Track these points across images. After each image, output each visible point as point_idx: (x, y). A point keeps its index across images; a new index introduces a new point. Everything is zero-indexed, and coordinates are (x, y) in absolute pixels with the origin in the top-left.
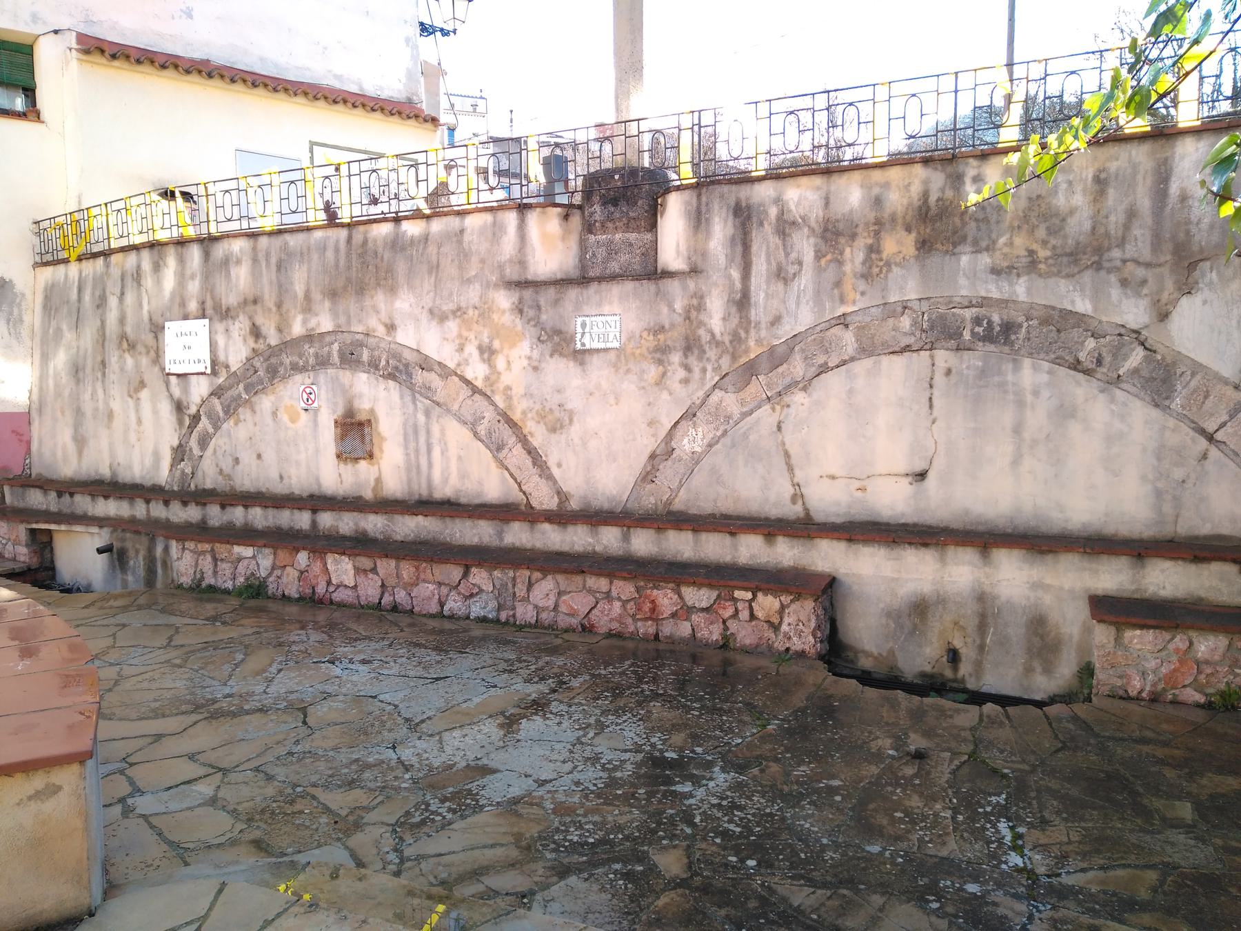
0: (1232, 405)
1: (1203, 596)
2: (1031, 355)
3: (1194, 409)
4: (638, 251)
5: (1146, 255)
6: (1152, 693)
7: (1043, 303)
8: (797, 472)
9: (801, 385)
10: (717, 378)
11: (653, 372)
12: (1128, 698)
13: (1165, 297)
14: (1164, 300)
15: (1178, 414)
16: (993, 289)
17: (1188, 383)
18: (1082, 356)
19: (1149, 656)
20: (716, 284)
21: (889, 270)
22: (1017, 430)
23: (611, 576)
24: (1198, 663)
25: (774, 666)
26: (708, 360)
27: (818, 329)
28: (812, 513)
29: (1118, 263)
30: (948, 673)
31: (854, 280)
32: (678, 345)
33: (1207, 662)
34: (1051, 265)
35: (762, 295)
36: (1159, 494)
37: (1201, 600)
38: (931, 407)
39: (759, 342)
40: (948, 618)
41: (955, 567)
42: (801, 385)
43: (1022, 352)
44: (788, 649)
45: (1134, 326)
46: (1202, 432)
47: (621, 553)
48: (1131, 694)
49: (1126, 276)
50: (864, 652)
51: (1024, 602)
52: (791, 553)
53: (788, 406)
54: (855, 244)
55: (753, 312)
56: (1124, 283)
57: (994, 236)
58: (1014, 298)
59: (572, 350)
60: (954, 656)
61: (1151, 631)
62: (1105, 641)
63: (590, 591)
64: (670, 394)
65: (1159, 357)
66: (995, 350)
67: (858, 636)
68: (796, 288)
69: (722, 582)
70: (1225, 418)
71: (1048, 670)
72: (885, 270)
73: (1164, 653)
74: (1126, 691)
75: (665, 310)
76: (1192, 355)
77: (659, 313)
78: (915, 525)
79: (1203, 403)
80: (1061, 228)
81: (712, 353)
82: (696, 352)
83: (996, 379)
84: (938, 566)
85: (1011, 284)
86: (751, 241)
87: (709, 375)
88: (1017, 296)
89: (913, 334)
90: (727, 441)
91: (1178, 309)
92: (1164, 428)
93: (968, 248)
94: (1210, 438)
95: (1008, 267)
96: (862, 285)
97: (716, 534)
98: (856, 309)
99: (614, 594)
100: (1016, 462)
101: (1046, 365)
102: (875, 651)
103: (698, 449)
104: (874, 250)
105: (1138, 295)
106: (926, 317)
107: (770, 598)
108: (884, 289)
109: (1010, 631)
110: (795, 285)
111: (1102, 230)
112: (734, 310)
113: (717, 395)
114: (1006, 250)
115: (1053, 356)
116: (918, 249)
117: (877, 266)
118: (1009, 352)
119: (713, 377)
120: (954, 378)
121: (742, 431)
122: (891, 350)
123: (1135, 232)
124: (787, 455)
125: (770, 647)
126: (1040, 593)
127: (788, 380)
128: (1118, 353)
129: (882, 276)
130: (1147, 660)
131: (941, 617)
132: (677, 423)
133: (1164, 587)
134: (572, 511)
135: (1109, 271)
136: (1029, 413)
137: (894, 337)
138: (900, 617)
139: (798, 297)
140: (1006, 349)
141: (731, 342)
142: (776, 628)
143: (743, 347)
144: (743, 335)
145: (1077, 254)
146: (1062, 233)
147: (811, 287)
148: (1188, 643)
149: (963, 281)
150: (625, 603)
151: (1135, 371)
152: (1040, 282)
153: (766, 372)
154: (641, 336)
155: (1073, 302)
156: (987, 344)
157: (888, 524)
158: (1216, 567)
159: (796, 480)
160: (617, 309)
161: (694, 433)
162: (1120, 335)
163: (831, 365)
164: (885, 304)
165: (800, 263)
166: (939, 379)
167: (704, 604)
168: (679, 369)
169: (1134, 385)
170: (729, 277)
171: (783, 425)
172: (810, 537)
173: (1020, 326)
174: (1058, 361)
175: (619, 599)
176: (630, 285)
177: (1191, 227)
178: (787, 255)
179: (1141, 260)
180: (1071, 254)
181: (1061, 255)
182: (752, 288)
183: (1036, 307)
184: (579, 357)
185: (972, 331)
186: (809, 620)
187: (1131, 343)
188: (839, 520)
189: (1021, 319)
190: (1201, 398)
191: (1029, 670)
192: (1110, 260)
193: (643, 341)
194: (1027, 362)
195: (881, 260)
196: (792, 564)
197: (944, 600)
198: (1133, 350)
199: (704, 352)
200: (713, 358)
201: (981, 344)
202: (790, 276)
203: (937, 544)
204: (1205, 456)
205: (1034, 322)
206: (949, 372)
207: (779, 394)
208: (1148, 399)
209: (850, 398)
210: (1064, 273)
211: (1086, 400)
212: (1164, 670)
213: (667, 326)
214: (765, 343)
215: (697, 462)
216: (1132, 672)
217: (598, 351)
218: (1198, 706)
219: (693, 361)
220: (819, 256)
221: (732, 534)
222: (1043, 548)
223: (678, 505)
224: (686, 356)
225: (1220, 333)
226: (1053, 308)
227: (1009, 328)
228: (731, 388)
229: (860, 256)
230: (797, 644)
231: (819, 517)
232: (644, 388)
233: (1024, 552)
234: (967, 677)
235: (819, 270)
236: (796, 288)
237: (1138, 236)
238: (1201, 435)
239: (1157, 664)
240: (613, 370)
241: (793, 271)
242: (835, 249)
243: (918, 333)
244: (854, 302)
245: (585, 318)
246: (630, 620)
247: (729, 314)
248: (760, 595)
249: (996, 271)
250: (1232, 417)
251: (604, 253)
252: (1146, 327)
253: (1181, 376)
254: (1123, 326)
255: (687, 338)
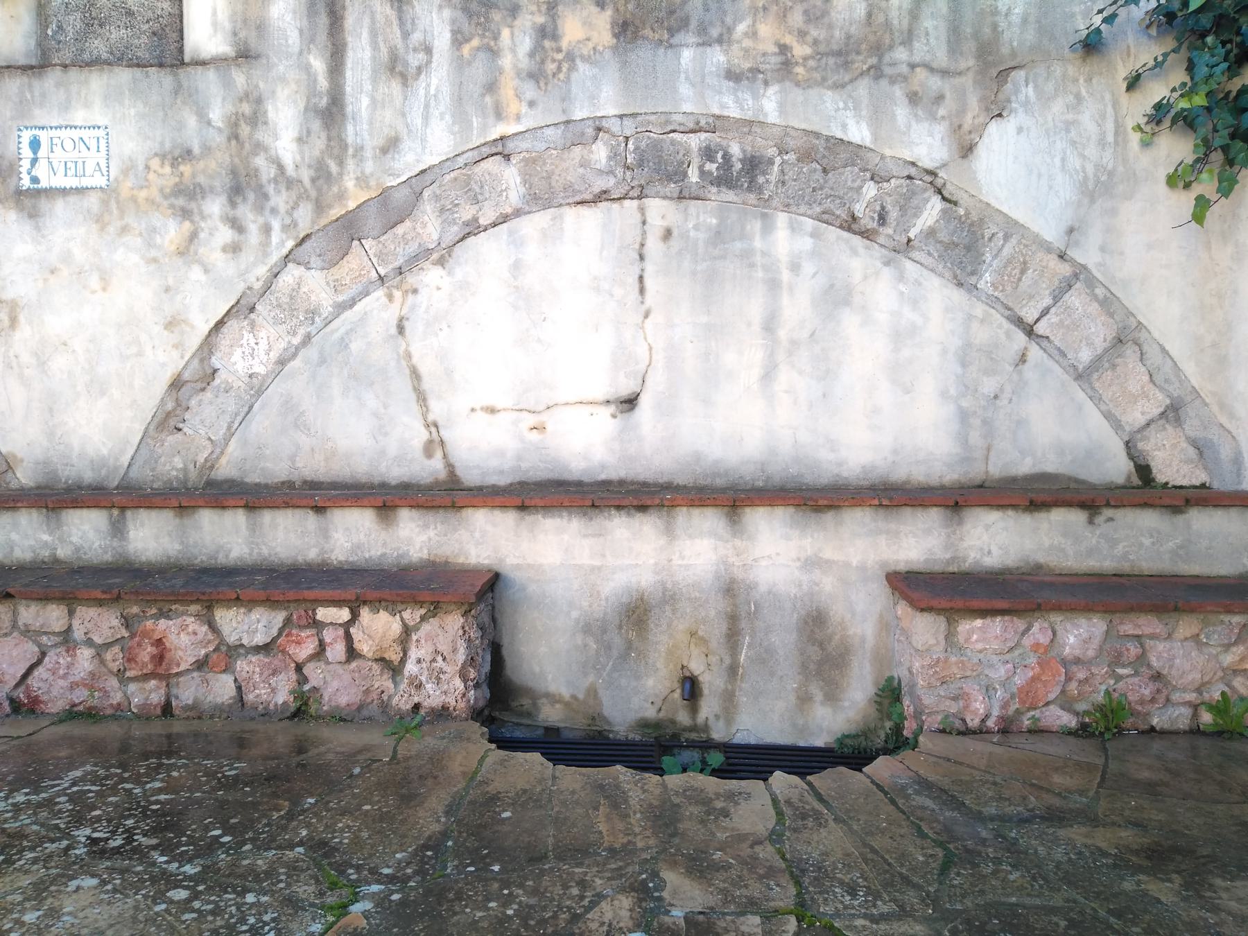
0: (1057, 283)
1: (1042, 560)
2: (787, 207)
3: (1009, 289)
4: (146, 27)
5: (941, 58)
6: (1002, 718)
7: (803, 126)
8: (433, 404)
9: (435, 256)
10: (290, 244)
11: (172, 231)
12: (966, 732)
13: (968, 121)
14: (966, 127)
15: (988, 296)
16: (730, 104)
17: (1000, 250)
18: (859, 209)
19: (995, 659)
20: (283, 80)
21: (573, 68)
22: (769, 326)
23: (70, 600)
24: (1064, 662)
25: (389, 743)
26: (274, 211)
27: (461, 161)
28: (459, 472)
29: (904, 69)
30: (683, 718)
31: (516, 82)
32: (217, 183)
33: (1077, 661)
34: (812, 69)
35: (365, 101)
36: (964, 416)
37: (1039, 567)
38: (642, 291)
39: (362, 181)
40: (682, 626)
41: (688, 542)
42: (435, 256)
43: (775, 203)
44: (417, 707)
45: (928, 164)
46: (1019, 322)
47: (108, 557)
48: (970, 724)
49: (916, 88)
50: (547, 695)
51: (794, 591)
52: (424, 538)
53: (415, 291)
54: (517, 23)
55: (350, 129)
56: (914, 99)
57: (729, 20)
58: (761, 119)
59: (12, 188)
60: (691, 688)
61: (998, 619)
62: (933, 641)
63: (27, 632)
64: (206, 271)
65: (962, 212)
66: (735, 199)
67: (537, 669)
68: (422, 92)
69: (291, 595)
70: (1047, 301)
71: (832, 697)
72: (565, 67)
73: (1017, 652)
74: (964, 720)
75: (192, 121)
76: (1005, 209)
77: (181, 126)
78: (622, 482)
79: (1020, 279)
80: (825, 13)
81: (280, 200)
82: (251, 196)
83: (738, 245)
84: (662, 541)
85: (756, 97)
86: (344, 8)
87: (276, 237)
88: (766, 115)
89: (611, 172)
90: (311, 352)
91: (985, 139)
92: (970, 317)
93: (691, 39)
94: (1029, 331)
95: (751, 70)
96: (530, 91)
97: (289, 512)
98: (521, 128)
99: (78, 634)
100: (768, 376)
101: (809, 223)
102: (566, 693)
103: (260, 369)
104: (547, 33)
105: (933, 117)
106: (631, 146)
107: (383, 616)
108: (566, 98)
109: (774, 639)
110: (421, 86)
111: (881, 18)
112: (316, 125)
113: (292, 274)
114: (747, 43)
115: (818, 209)
116: (616, 36)
117: (554, 61)
118: (755, 202)
119: (283, 243)
120: (675, 243)
121: (337, 335)
122: (578, 199)
123: (926, 24)
124: (415, 374)
125: (385, 706)
126: (817, 574)
127: (412, 248)
128: (908, 207)
129: (561, 76)
130: (992, 666)
131: (669, 626)
132: (220, 324)
133: (989, 552)
134: (22, 489)
135: (893, 80)
136: (785, 300)
137: (583, 177)
138: (604, 631)
139: (427, 106)
140: (752, 198)
141: (313, 180)
142: (394, 669)
143: (335, 189)
144: (333, 167)
145: (847, 53)
146: (826, 20)
147: (446, 90)
148: (1050, 632)
149: (685, 90)
150: (100, 650)
151: (931, 233)
152: (797, 95)
153: (375, 233)
154: (147, 167)
155: (844, 126)
156: (724, 189)
157: (579, 484)
158: (1058, 516)
159: (431, 418)
160: (99, 116)
161: (252, 341)
162: (909, 177)
163: (483, 221)
164: (568, 122)
165: (428, 50)
166: (654, 245)
167: (260, 639)
168: (221, 226)
169: (929, 254)
170: (307, 68)
171: (406, 324)
172: (455, 507)
173: (771, 162)
174: (825, 218)
175: (89, 643)
176: (124, 75)
177: (998, 18)
178: (406, 35)
179: (935, 65)
180: (839, 53)
181: (827, 54)
182: (348, 89)
183: (793, 133)
184: (27, 202)
185: (701, 168)
186: (455, 650)
187: (925, 190)
188: (503, 481)
189: (772, 152)
190: (1017, 271)
191: (804, 700)
192: (893, 64)
193: (151, 176)
194: (782, 219)
195: (559, 50)
196: (424, 555)
197: (673, 597)
198: (927, 200)
199: (266, 197)
200: (283, 208)
201: (714, 189)
202: (413, 71)
203: (661, 506)
204: (1023, 359)
205: (791, 157)
206: (668, 234)
207: (400, 271)
208: (948, 274)
209: (515, 278)
210: (830, 82)
211: (865, 278)
212: (1019, 680)
213: (196, 150)
214: (373, 183)
215: (260, 393)
216: (973, 689)
217: (64, 192)
218: (1071, 733)
219: (245, 212)
220: (459, 39)
221: (319, 509)
222: (821, 502)
223: (226, 469)
224: (233, 204)
225: (1040, 176)
226: (817, 135)
227: (754, 165)
228: (315, 261)
229: (526, 44)
230: (433, 696)
231: (470, 477)
232: (155, 260)
233: (791, 510)
234: (711, 722)
235: (460, 64)
236: (422, 92)
237: (931, 30)
238: (1019, 327)
239: (1007, 671)
240: (95, 227)
241: (416, 63)
242: (485, 30)
243: (619, 171)
244: (518, 118)
245: (37, 132)
246: (114, 682)
247: (309, 132)
248: (365, 613)
249: (733, 76)
250: (1056, 299)
251: (79, 25)
252: (944, 165)
253: (990, 239)
254: (913, 164)
255: (234, 172)
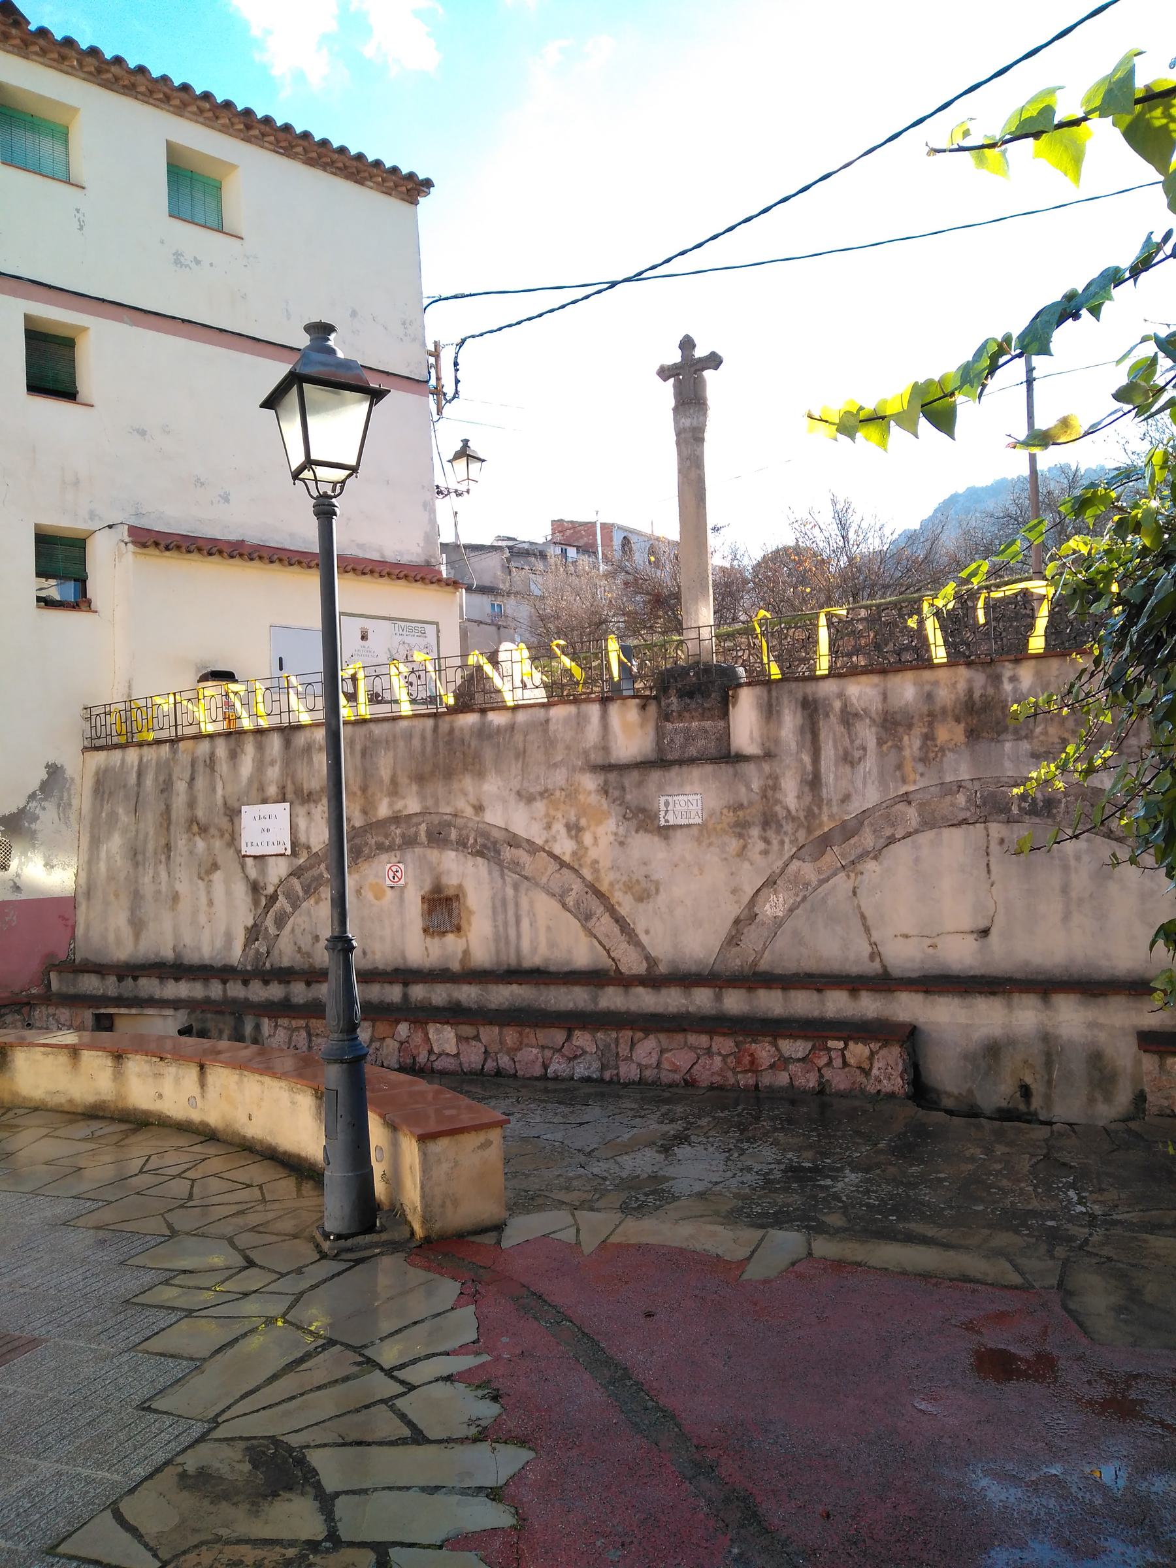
10: (794, 850)
11: (734, 844)
21: (944, 755)
22: (1065, 890)
23: (711, 1033)
26: (786, 833)
27: (884, 805)
30: (1022, 1107)
35: (832, 776)
38: (989, 872)
39: (831, 817)
44: (879, 1091)
47: (714, 1012)
50: (946, 1093)
52: (874, 1006)
53: (862, 873)
55: (824, 790)
60: (1026, 1091)
62: (1152, 1068)
63: (692, 1048)
64: (752, 864)
66: (1040, 822)
67: (939, 1078)
71: (1108, 1098)
74: (1173, 1110)
75: (743, 790)
78: (983, 977)
81: (788, 827)
82: (774, 826)
87: (787, 846)
89: (968, 809)
90: (807, 905)
93: (1010, 737)
95: (1045, 752)
96: (920, 768)
99: (715, 1049)
100: (1066, 917)
102: (956, 1091)
103: (780, 914)
104: (929, 737)
108: (941, 771)
112: (806, 789)
113: (795, 865)
114: (1042, 738)
116: (967, 737)
122: (949, 823)
125: (862, 1091)
127: (859, 851)
129: (938, 760)
132: (759, 890)
134: (661, 975)
139: (865, 777)
140: (1050, 821)
141: (806, 817)
142: (867, 1073)
143: (817, 822)
144: (816, 810)
149: (1008, 764)
150: (725, 1057)
157: (958, 977)
159: (873, 940)
160: (697, 788)
161: (775, 899)
164: (942, 784)
165: (865, 749)
166: (994, 848)
167: (800, 1055)
170: (801, 760)
171: (857, 890)
173: (1060, 801)
175: (719, 1054)
176: (709, 768)
178: (852, 742)
182: (823, 771)
184: (663, 832)
185: (1019, 806)
186: (897, 1064)
188: (914, 975)
189: (1060, 796)
191: (1091, 1100)
192: (1129, 747)
195: (936, 746)
196: (875, 1015)
199: (781, 826)
200: (790, 831)
201: (1028, 817)
203: (1004, 992)
207: (853, 863)
213: (746, 804)
214: (837, 818)
215: (780, 926)
217: (681, 826)
219: (771, 834)
220: (880, 742)
221: (819, 991)
223: (763, 966)
224: (764, 830)
228: (807, 858)
229: (917, 743)
230: (887, 1086)
231: (896, 972)
232: (726, 859)
234: (1039, 1111)
235: (881, 755)
236: (862, 771)
240: (696, 843)
243: (973, 809)
244: (915, 782)
246: (730, 1074)
248: (851, 1044)
251: (682, 740)
255: (764, 814)
